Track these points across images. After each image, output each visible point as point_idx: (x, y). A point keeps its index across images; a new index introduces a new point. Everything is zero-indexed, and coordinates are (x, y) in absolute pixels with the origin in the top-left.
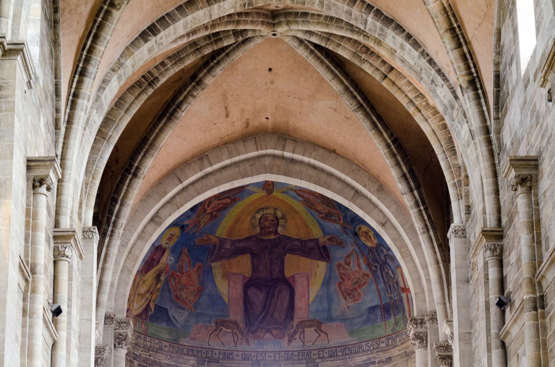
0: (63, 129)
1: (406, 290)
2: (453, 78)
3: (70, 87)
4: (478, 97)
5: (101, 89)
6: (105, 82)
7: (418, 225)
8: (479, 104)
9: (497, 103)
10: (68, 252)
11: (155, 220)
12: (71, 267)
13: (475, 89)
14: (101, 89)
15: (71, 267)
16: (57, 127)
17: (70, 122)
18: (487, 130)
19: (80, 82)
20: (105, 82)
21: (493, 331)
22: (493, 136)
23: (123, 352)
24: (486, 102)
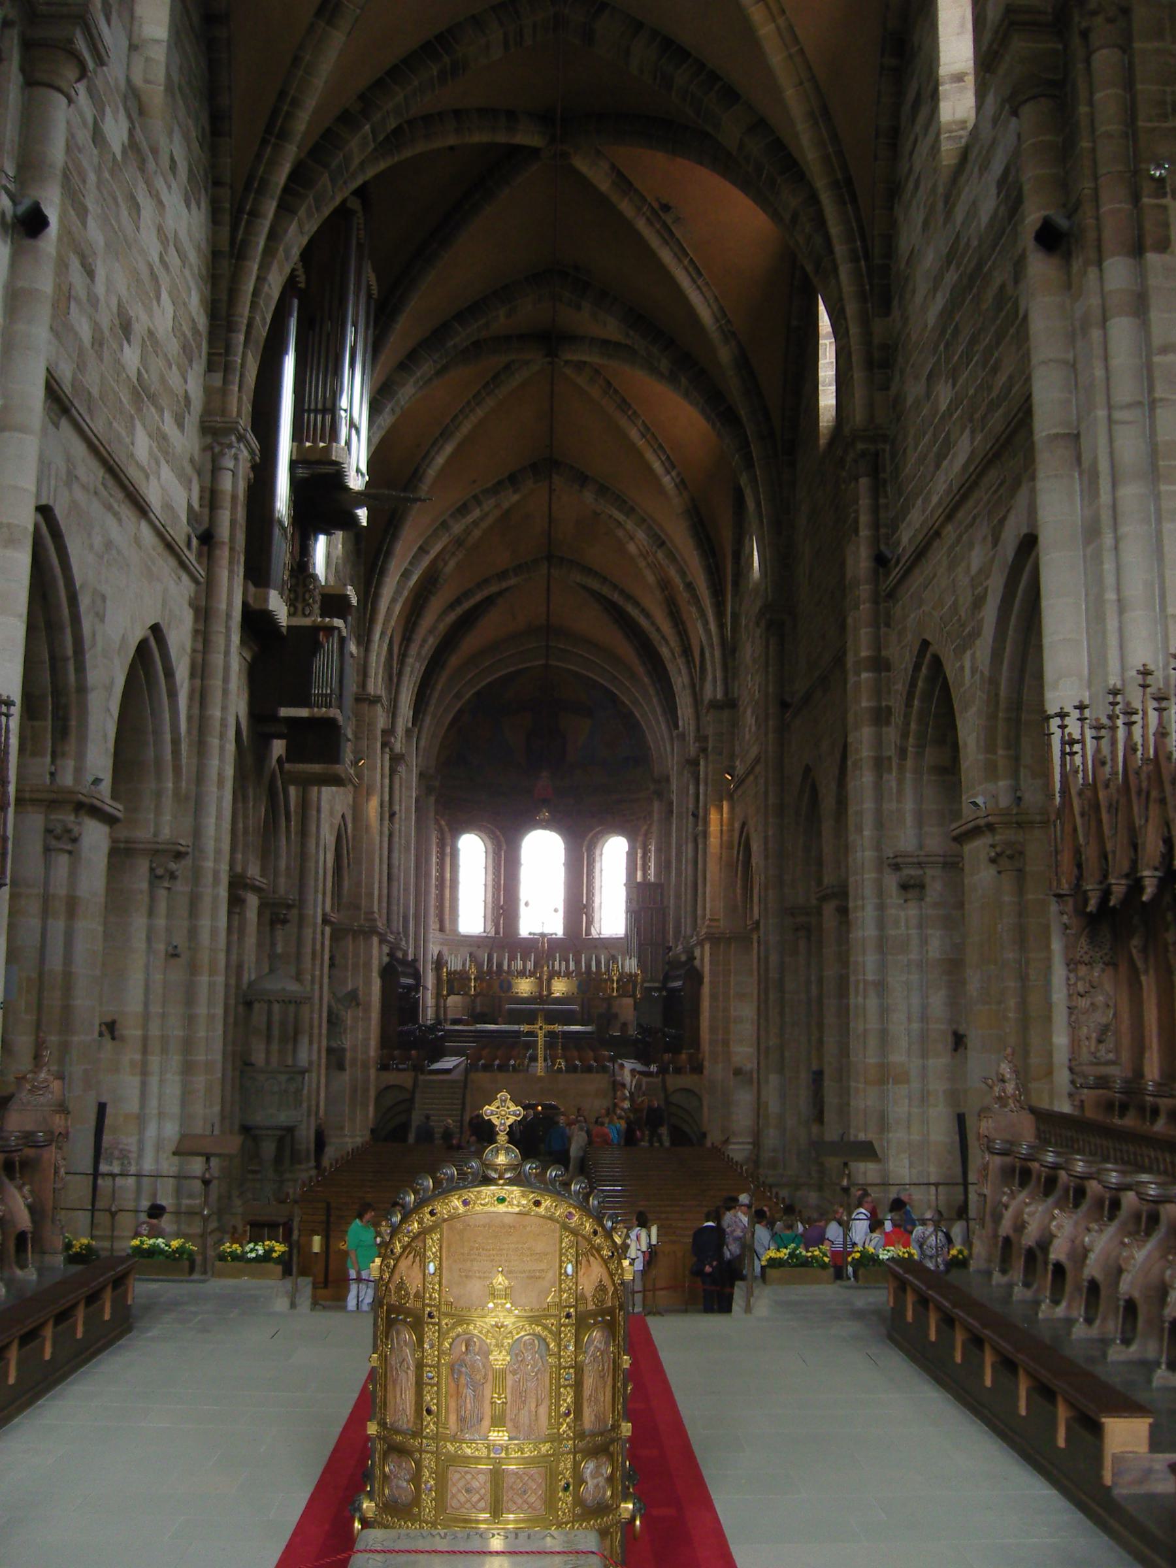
0: (395, 680)
1: (650, 748)
2: (673, 644)
3: (400, 649)
4: (688, 662)
5: (422, 646)
6: (424, 641)
7: (659, 711)
8: (689, 668)
9: (701, 668)
10: (399, 769)
11: (458, 696)
12: (401, 778)
13: (687, 657)
14: (422, 646)
15: (401, 778)
16: (390, 679)
17: (400, 674)
18: (693, 685)
19: (407, 647)
20: (424, 641)
21: (690, 830)
22: (697, 689)
23: (432, 799)
24: (695, 667)
